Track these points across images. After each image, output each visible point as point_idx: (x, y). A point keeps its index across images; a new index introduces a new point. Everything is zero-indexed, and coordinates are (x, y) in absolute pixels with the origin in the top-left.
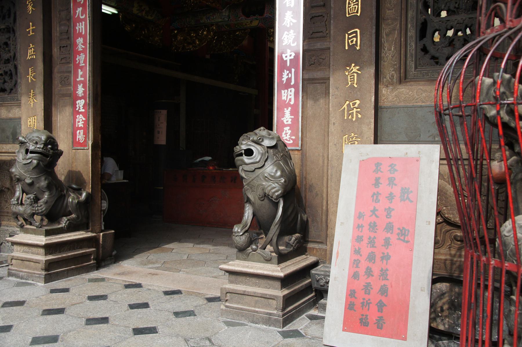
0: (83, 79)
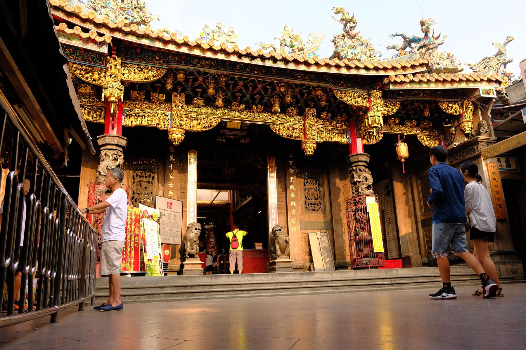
0: (193, 205)
